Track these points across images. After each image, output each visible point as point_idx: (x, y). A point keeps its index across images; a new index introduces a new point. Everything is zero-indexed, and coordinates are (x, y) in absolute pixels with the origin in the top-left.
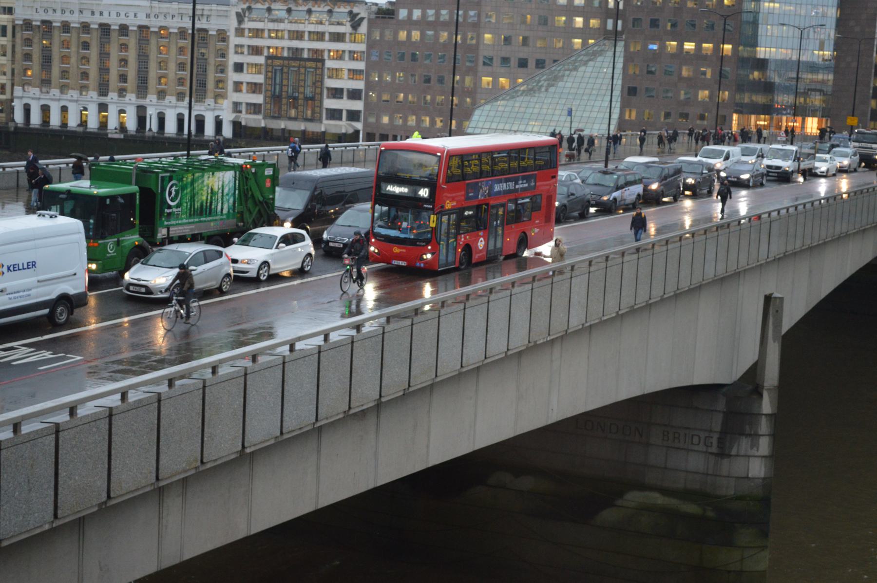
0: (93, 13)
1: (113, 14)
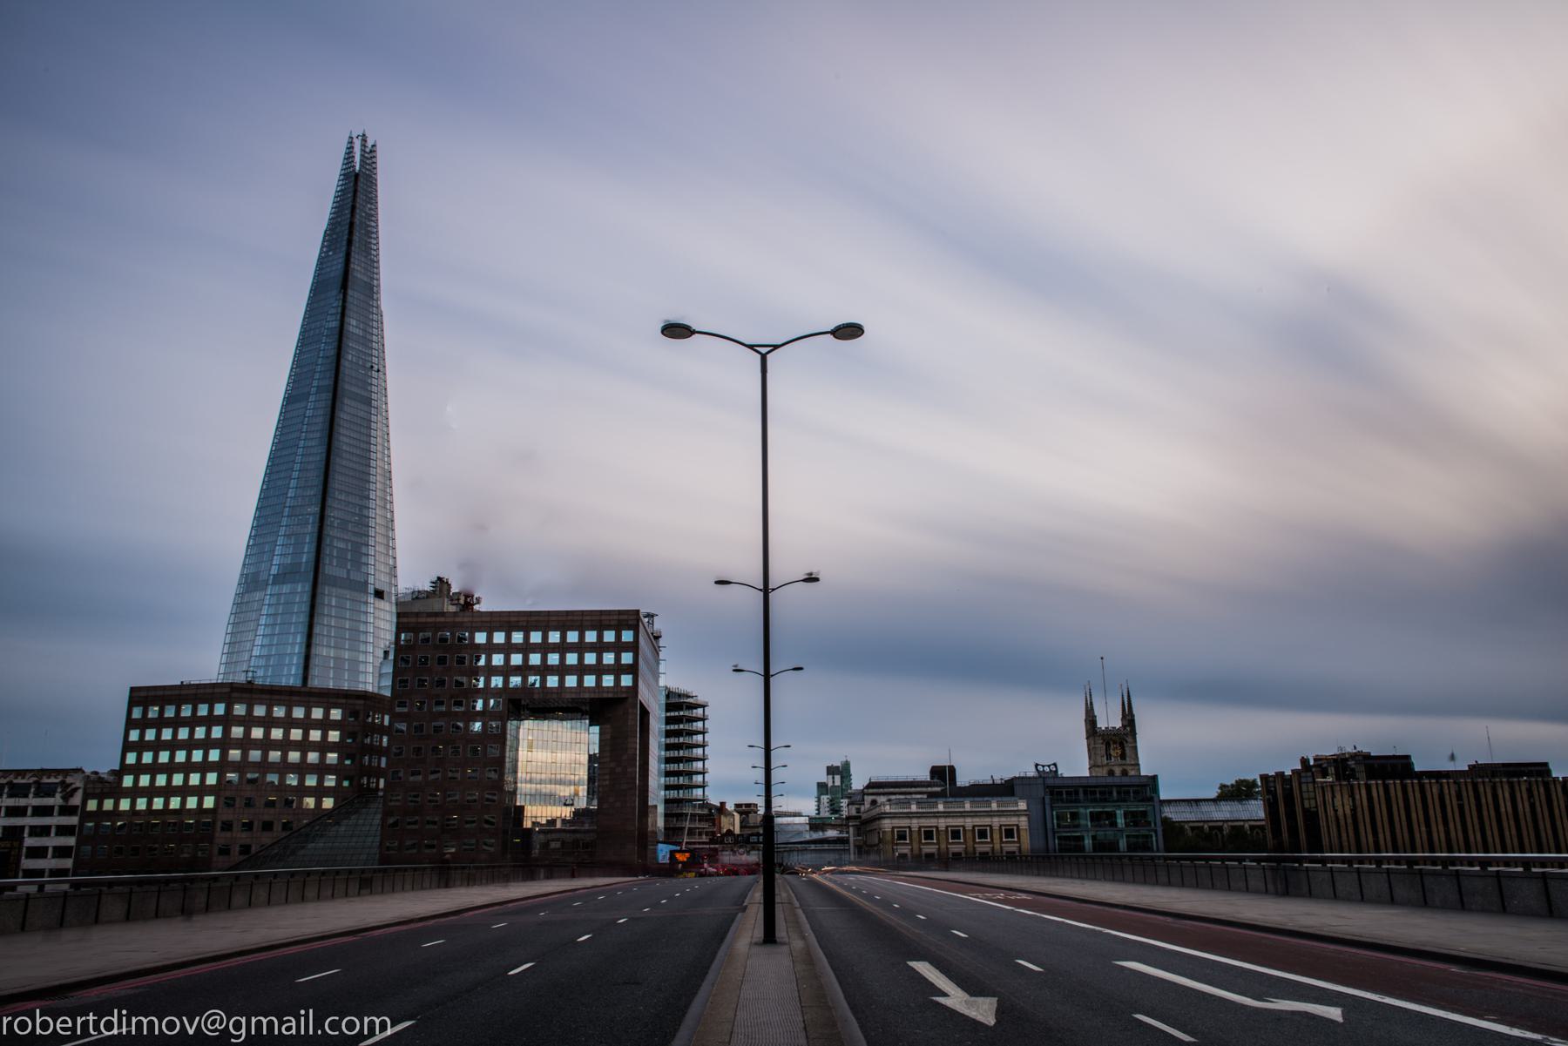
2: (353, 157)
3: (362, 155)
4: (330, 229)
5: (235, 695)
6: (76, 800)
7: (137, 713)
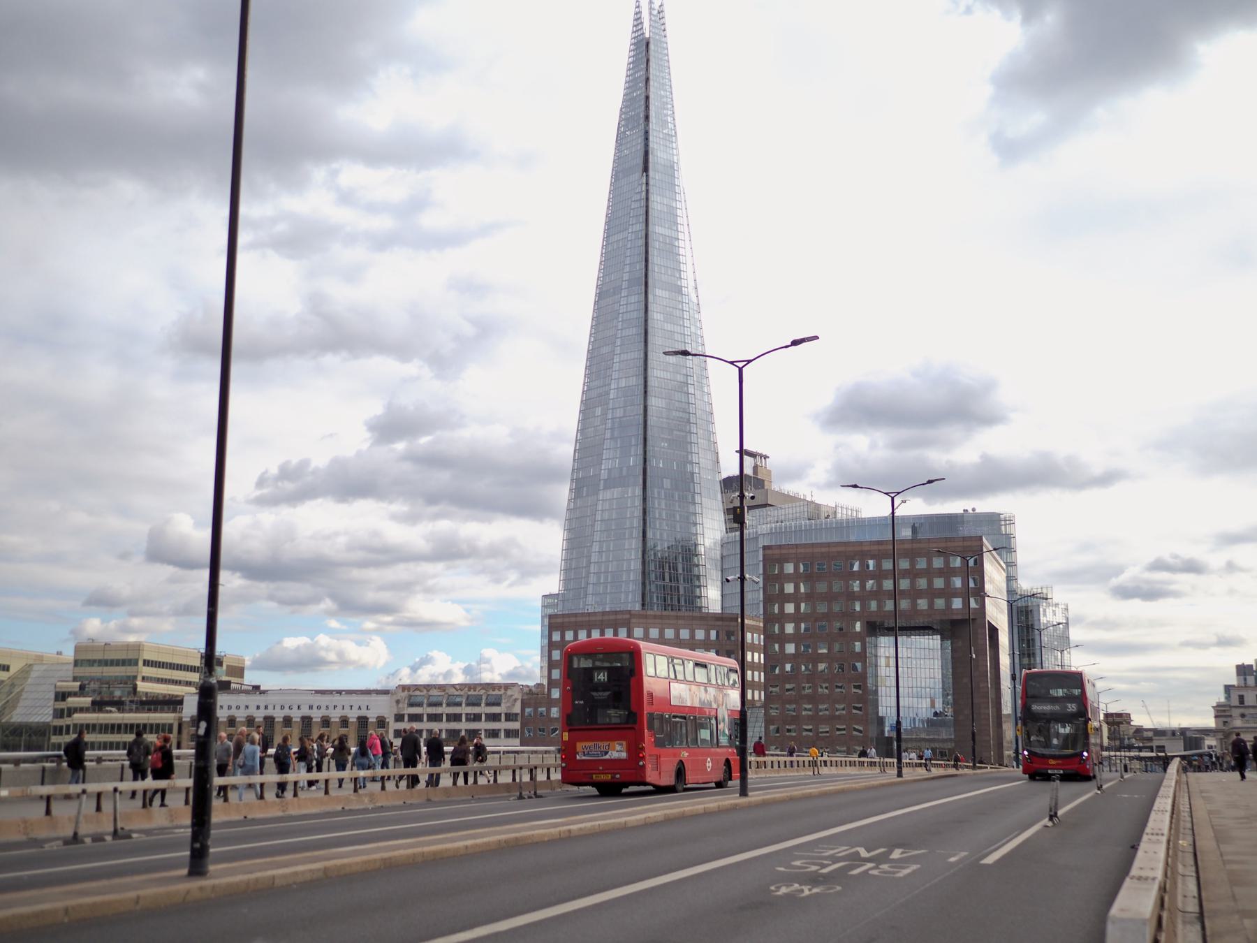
0: (258, 707)
1: (278, 707)
2: (642, 23)
3: (651, 20)
4: (626, 107)
5: (633, 620)
6: (517, 709)
7: (556, 637)
